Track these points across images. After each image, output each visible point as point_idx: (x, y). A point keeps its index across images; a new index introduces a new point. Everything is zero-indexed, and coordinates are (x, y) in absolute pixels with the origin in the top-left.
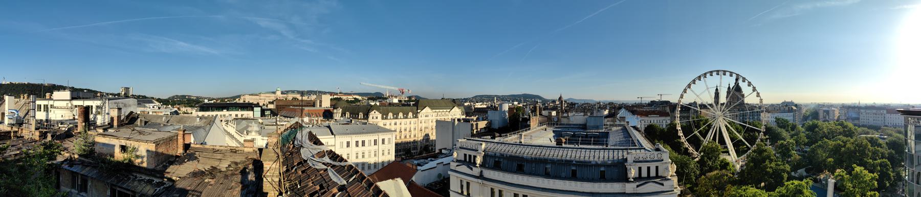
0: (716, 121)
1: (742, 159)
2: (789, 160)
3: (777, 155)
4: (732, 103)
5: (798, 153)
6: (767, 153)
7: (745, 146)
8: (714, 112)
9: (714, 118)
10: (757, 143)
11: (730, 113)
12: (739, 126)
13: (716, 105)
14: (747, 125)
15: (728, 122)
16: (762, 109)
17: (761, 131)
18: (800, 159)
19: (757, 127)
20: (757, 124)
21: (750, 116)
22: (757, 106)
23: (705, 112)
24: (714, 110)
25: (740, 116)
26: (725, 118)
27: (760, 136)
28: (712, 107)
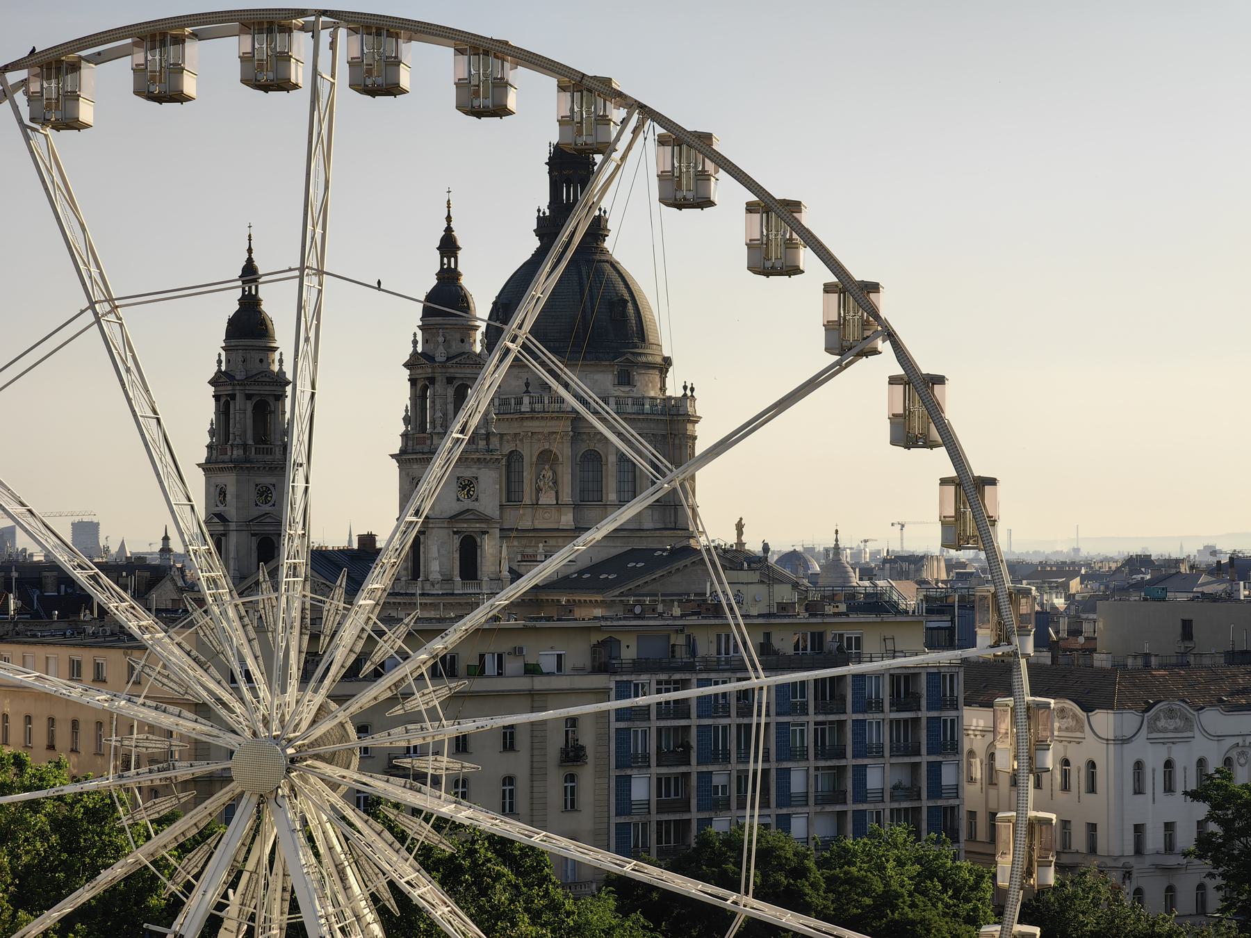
0: (242, 823)
4: (491, 550)
8: (206, 684)
9: (206, 785)
11: (456, 705)
13: (244, 583)
14: (748, 906)
15: (427, 860)
16: (984, 645)
20: (900, 878)
21: (787, 749)
22: (907, 595)
23: (57, 684)
24: (207, 656)
25: (628, 758)
26: (380, 785)
28: (171, 616)
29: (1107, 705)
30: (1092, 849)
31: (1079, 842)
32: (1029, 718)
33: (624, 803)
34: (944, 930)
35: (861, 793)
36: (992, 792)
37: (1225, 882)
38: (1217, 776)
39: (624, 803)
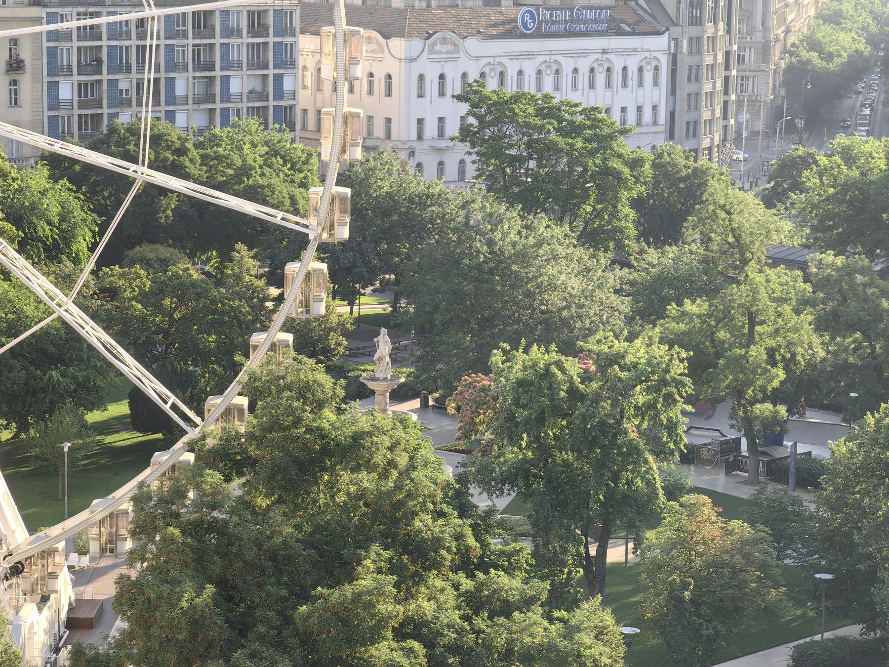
1: (78, 546)
2: (616, 554)
3: (481, 501)
5: (720, 482)
6: (367, 480)
7: (121, 409)
10: (253, 364)
12: (39, 178)
17: (297, 244)
18: (743, 548)
19: (254, 194)
20: (254, 156)
27: (293, 292)
29: (400, 34)
30: (388, 136)
31: (379, 130)
32: (345, 41)
33: (54, 102)
34: (285, 190)
35: (226, 96)
36: (319, 95)
37: (478, 158)
38: (475, 84)
39: (54, 102)
